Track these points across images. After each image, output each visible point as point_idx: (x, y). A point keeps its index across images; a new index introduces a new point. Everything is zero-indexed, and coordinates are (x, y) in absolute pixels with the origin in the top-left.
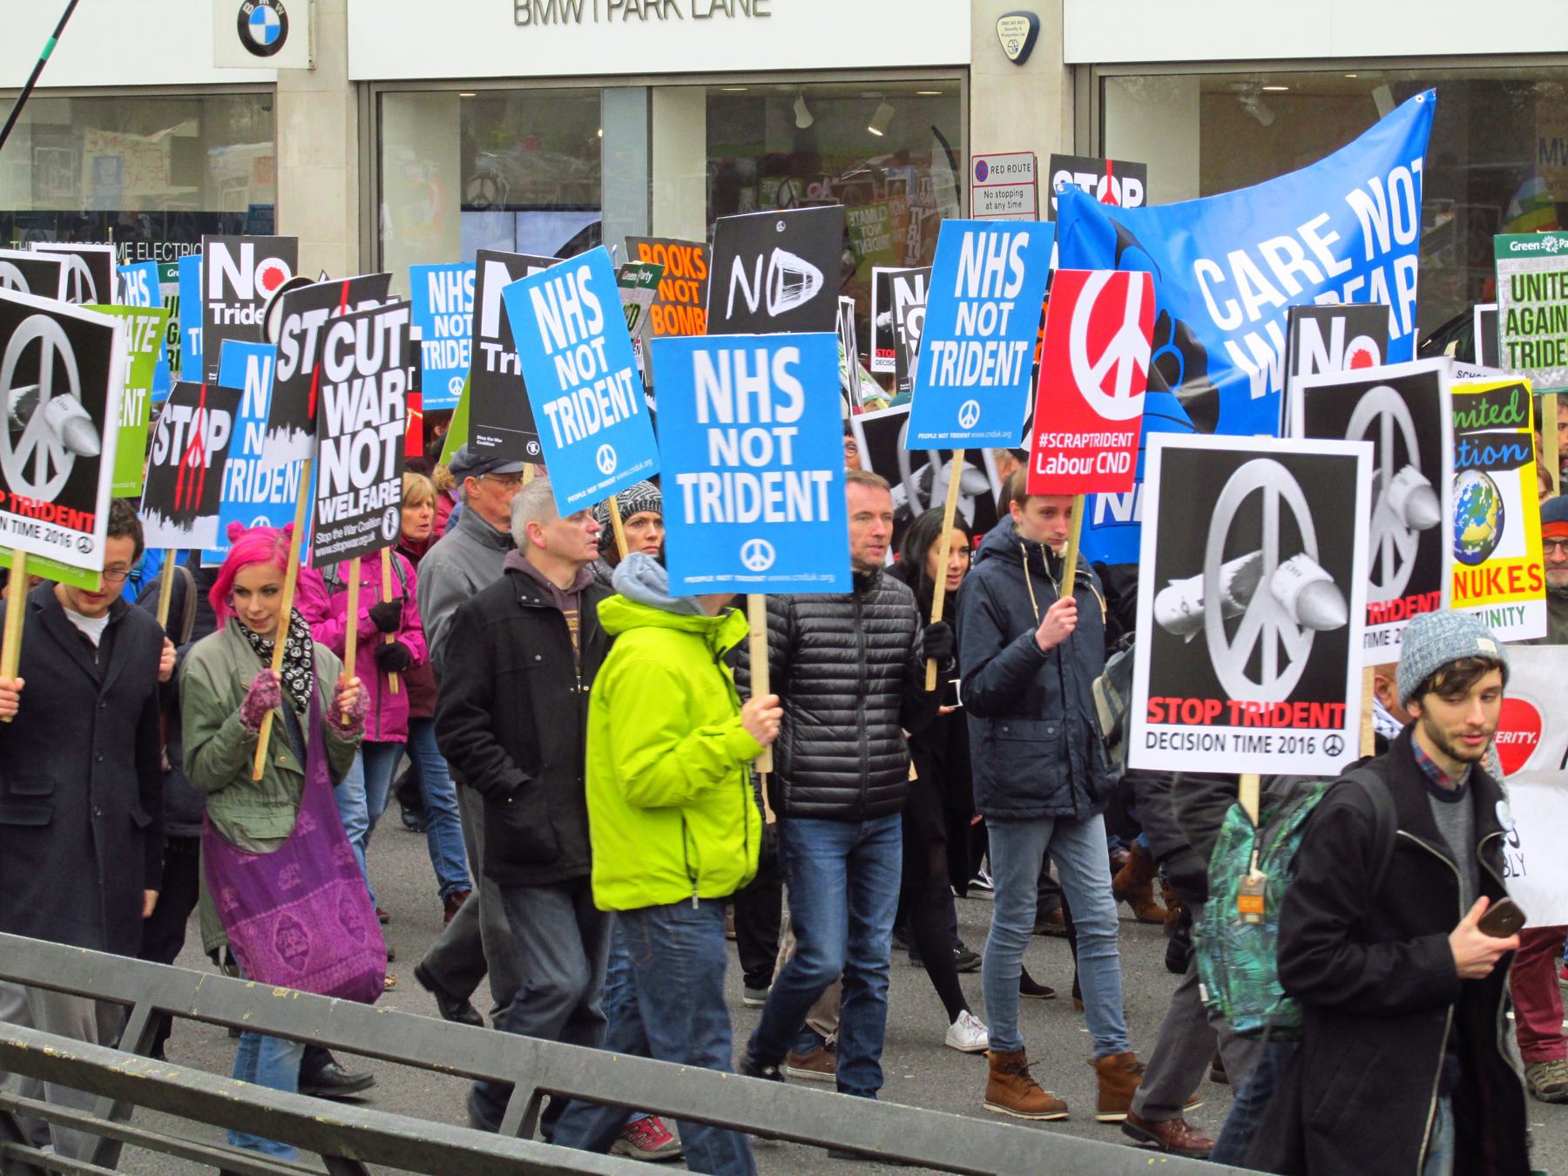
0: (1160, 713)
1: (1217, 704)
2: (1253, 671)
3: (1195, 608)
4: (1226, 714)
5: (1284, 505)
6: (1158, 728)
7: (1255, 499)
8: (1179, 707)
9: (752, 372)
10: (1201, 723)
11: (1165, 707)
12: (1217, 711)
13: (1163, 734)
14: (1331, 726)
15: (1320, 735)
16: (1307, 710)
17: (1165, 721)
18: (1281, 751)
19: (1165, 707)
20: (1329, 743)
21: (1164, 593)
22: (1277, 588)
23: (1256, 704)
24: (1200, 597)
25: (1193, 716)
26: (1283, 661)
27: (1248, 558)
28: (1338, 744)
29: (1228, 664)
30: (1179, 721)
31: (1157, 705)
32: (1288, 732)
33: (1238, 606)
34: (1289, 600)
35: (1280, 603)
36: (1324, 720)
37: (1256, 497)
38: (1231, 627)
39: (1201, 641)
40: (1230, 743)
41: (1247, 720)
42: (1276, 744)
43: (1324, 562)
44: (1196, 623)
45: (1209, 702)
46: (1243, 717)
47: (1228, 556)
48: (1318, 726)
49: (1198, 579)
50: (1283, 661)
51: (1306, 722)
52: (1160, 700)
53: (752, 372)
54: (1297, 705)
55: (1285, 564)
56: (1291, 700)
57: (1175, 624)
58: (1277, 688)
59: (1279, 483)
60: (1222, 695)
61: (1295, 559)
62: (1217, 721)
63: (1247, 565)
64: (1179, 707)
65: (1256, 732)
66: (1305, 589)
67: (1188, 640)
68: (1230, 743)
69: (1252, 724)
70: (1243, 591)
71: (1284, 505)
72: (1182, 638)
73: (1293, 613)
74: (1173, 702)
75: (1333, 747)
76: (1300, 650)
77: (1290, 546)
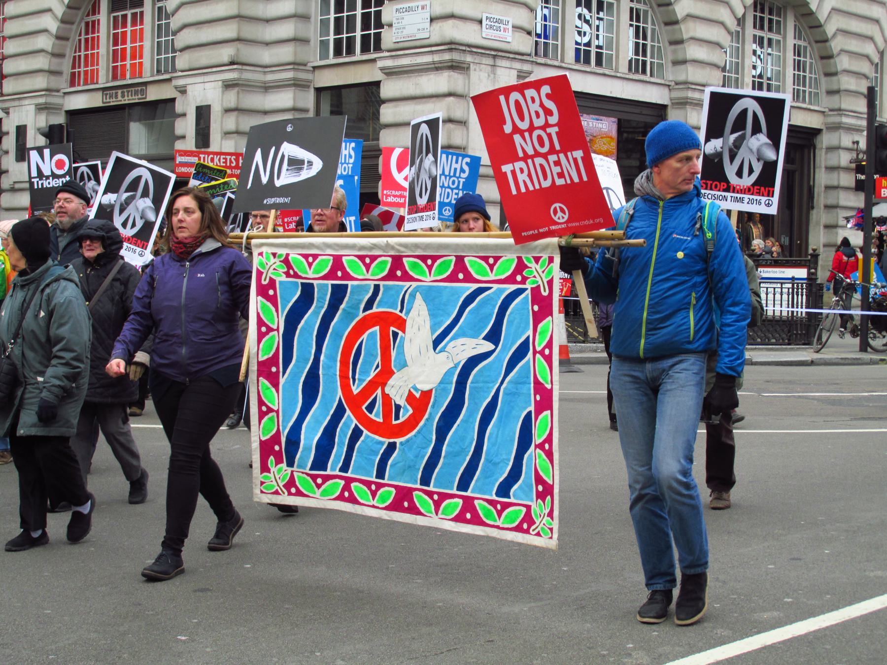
0: (704, 186)
1: (725, 185)
2: (739, 174)
3: (719, 149)
4: (729, 188)
5: (755, 115)
7: (744, 112)
8: (711, 185)
9: (457, 162)
10: (719, 191)
11: (706, 184)
12: (725, 188)
14: (768, 196)
15: (763, 199)
16: (760, 189)
18: (748, 203)
19: (706, 184)
20: (767, 202)
22: (750, 145)
23: (740, 186)
25: (716, 188)
26: (751, 171)
28: (770, 203)
29: (730, 171)
30: (711, 189)
32: (751, 197)
34: (755, 150)
35: (751, 150)
36: (766, 194)
37: (744, 112)
40: (729, 199)
41: (736, 191)
42: (746, 200)
43: (769, 136)
44: (719, 155)
45: (722, 184)
46: (734, 190)
48: (763, 195)
49: (721, 139)
50: (751, 171)
51: (759, 194)
53: (457, 162)
54: (755, 187)
55: (753, 137)
56: (753, 185)
57: (712, 155)
58: (748, 181)
59: (753, 107)
60: (727, 182)
61: (758, 135)
62: (724, 191)
64: (711, 185)
65: (739, 196)
66: (761, 146)
68: (729, 199)
69: (738, 192)
70: (738, 144)
73: (756, 154)
74: (709, 182)
75: (769, 203)
76: (758, 168)
77: (756, 130)
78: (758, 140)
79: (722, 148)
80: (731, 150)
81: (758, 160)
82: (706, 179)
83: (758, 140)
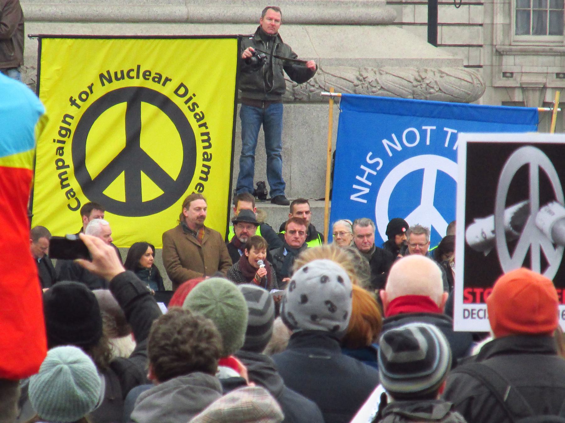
0: (471, 297)
3: (489, 235)
5: (542, 174)
6: (470, 306)
7: (524, 170)
11: (474, 294)
13: (472, 310)
17: (474, 301)
19: (474, 294)
21: (471, 227)
22: (539, 222)
24: (492, 228)
27: (520, 205)
31: (469, 293)
33: (515, 233)
35: (541, 231)
37: (524, 170)
38: (512, 246)
39: (494, 256)
47: (509, 203)
52: (470, 290)
55: (543, 209)
63: (521, 210)
67: (486, 254)
71: (542, 173)
72: (482, 253)
74: (478, 291)
78: (551, 212)
79: (493, 232)
80: (508, 235)
81: (555, 246)
82: (473, 287)
83: (551, 212)
